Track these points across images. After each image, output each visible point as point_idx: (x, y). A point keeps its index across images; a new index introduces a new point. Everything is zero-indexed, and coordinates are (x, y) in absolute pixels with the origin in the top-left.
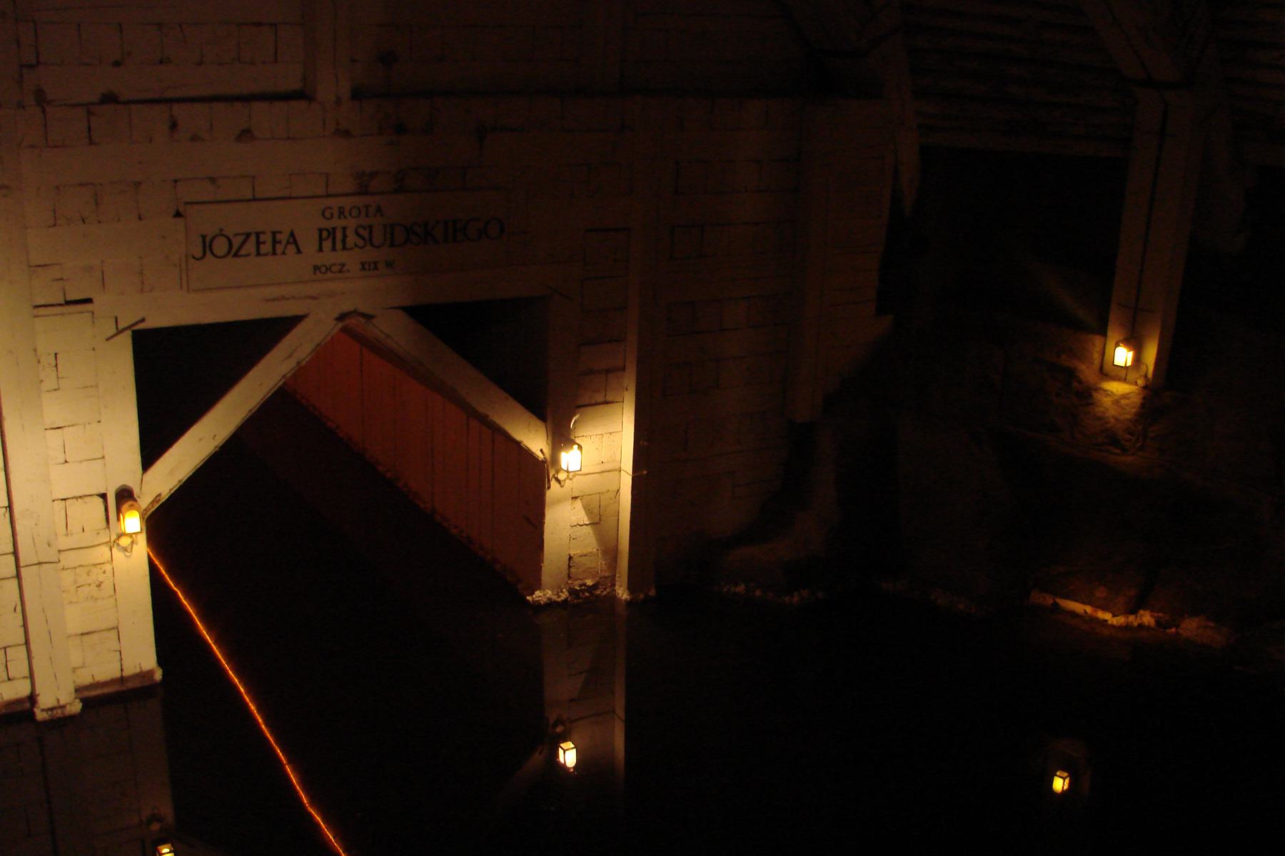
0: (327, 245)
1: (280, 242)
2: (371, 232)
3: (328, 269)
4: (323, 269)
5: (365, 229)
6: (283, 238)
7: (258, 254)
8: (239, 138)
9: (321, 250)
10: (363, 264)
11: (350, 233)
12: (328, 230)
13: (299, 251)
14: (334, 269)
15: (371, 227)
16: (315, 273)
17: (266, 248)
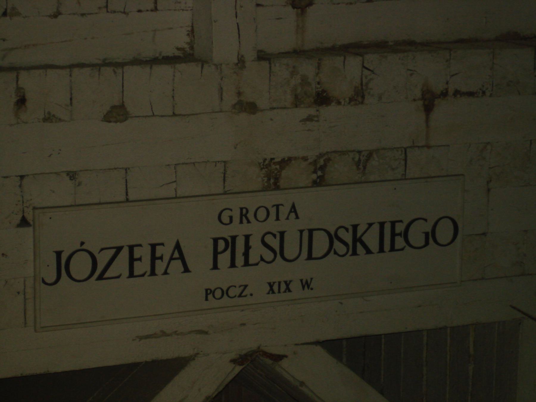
0: (224, 259)
3: (225, 293)
4: (218, 293)
6: (166, 251)
7: (131, 275)
8: (108, 118)
9: (215, 267)
10: (271, 285)
11: (255, 242)
12: (225, 240)
13: (186, 270)
14: (231, 293)
15: (282, 234)
16: (207, 299)
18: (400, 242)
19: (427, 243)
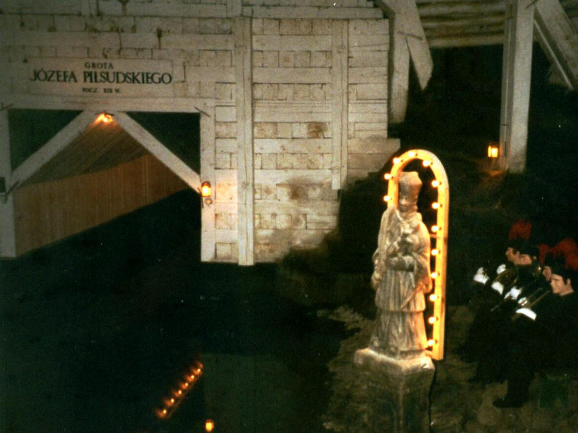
0: (88, 79)
1: (68, 76)
2: (108, 76)
5: (105, 73)
6: (69, 74)
9: (85, 81)
11: (98, 75)
15: (107, 73)
17: (62, 78)
18: (150, 80)
19: (160, 82)
